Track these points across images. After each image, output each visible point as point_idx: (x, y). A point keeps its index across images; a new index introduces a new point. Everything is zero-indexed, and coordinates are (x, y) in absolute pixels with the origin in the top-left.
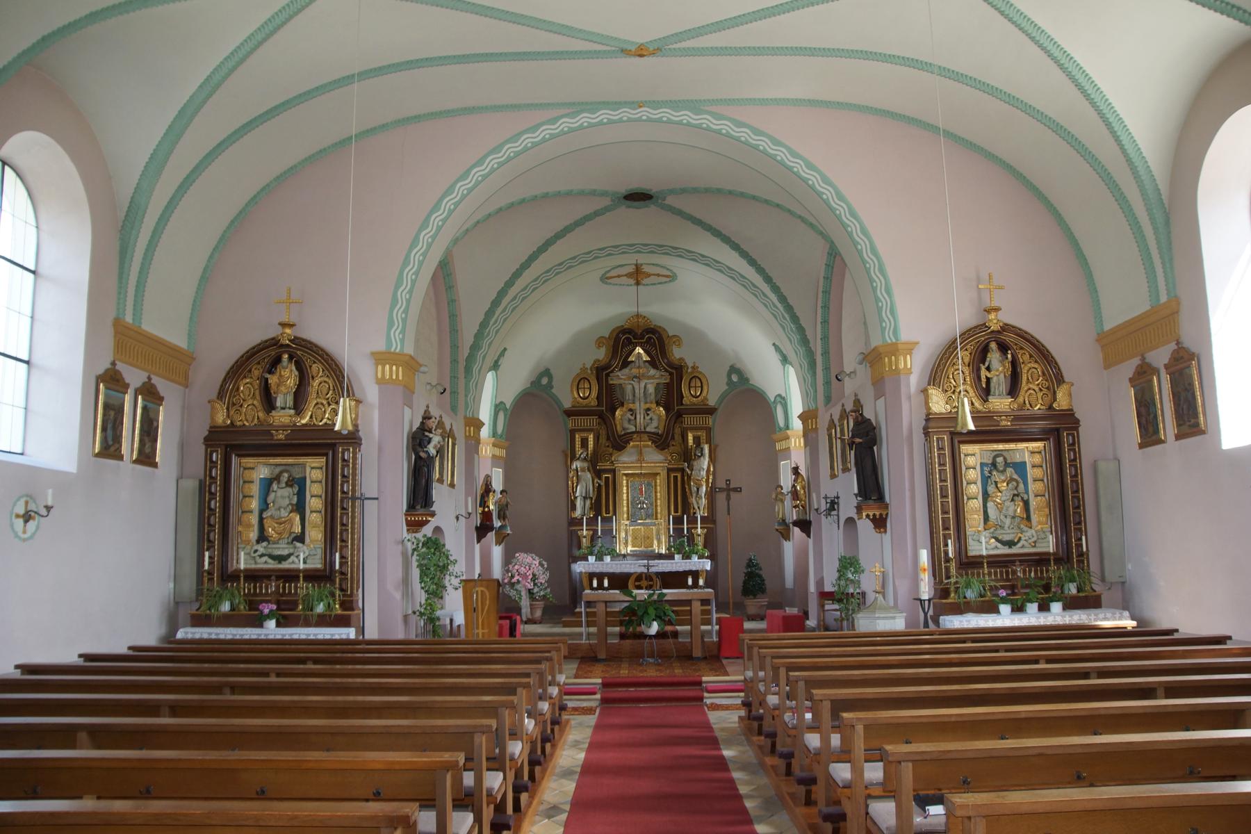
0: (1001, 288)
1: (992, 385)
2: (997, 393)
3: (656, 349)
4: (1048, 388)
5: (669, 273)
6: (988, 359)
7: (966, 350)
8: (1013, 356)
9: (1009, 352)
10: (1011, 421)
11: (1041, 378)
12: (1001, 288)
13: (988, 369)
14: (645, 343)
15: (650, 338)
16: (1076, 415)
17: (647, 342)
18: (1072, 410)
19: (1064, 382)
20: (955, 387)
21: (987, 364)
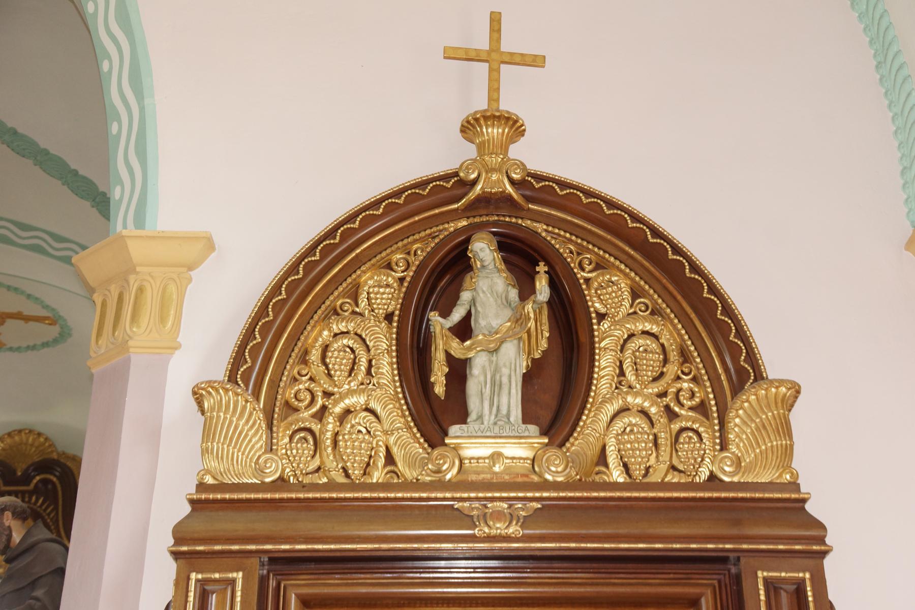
0: (536, 61)
1: (472, 387)
2: (489, 419)
3: (56, 508)
4: (702, 408)
5: (44, 313)
6: (465, 296)
7: (389, 266)
8: (554, 284)
9: (542, 268)
10: (525, 522)
11: (672, 369)
12: (536, 61)
13: (464, 330)
14: (31, 493)
15: (45, 482)
16: (808, 507)
17: (36, 491)
18: (794, 486)
19: (763, 378)
20: (327, 394)
21: (457, 315)
